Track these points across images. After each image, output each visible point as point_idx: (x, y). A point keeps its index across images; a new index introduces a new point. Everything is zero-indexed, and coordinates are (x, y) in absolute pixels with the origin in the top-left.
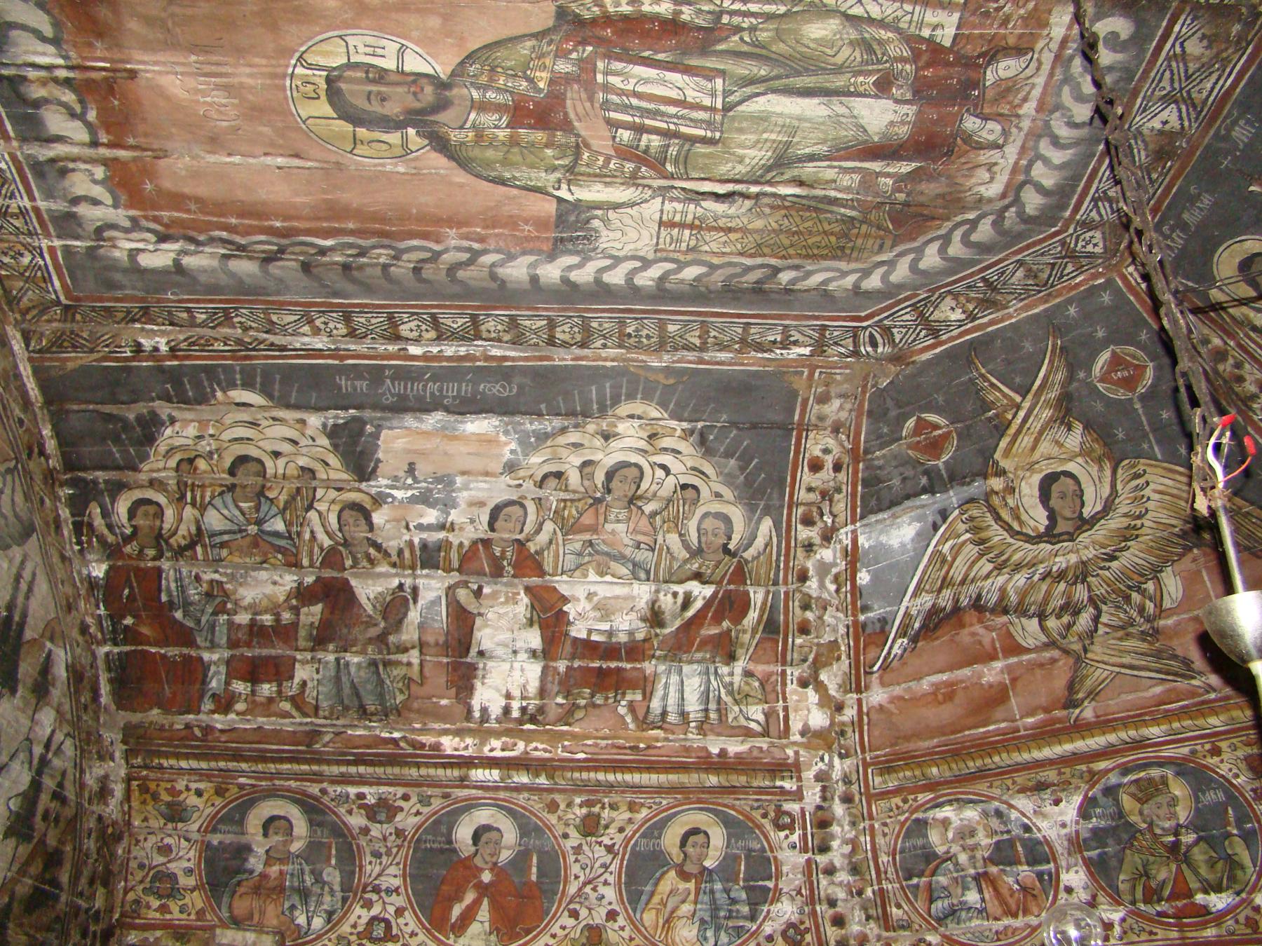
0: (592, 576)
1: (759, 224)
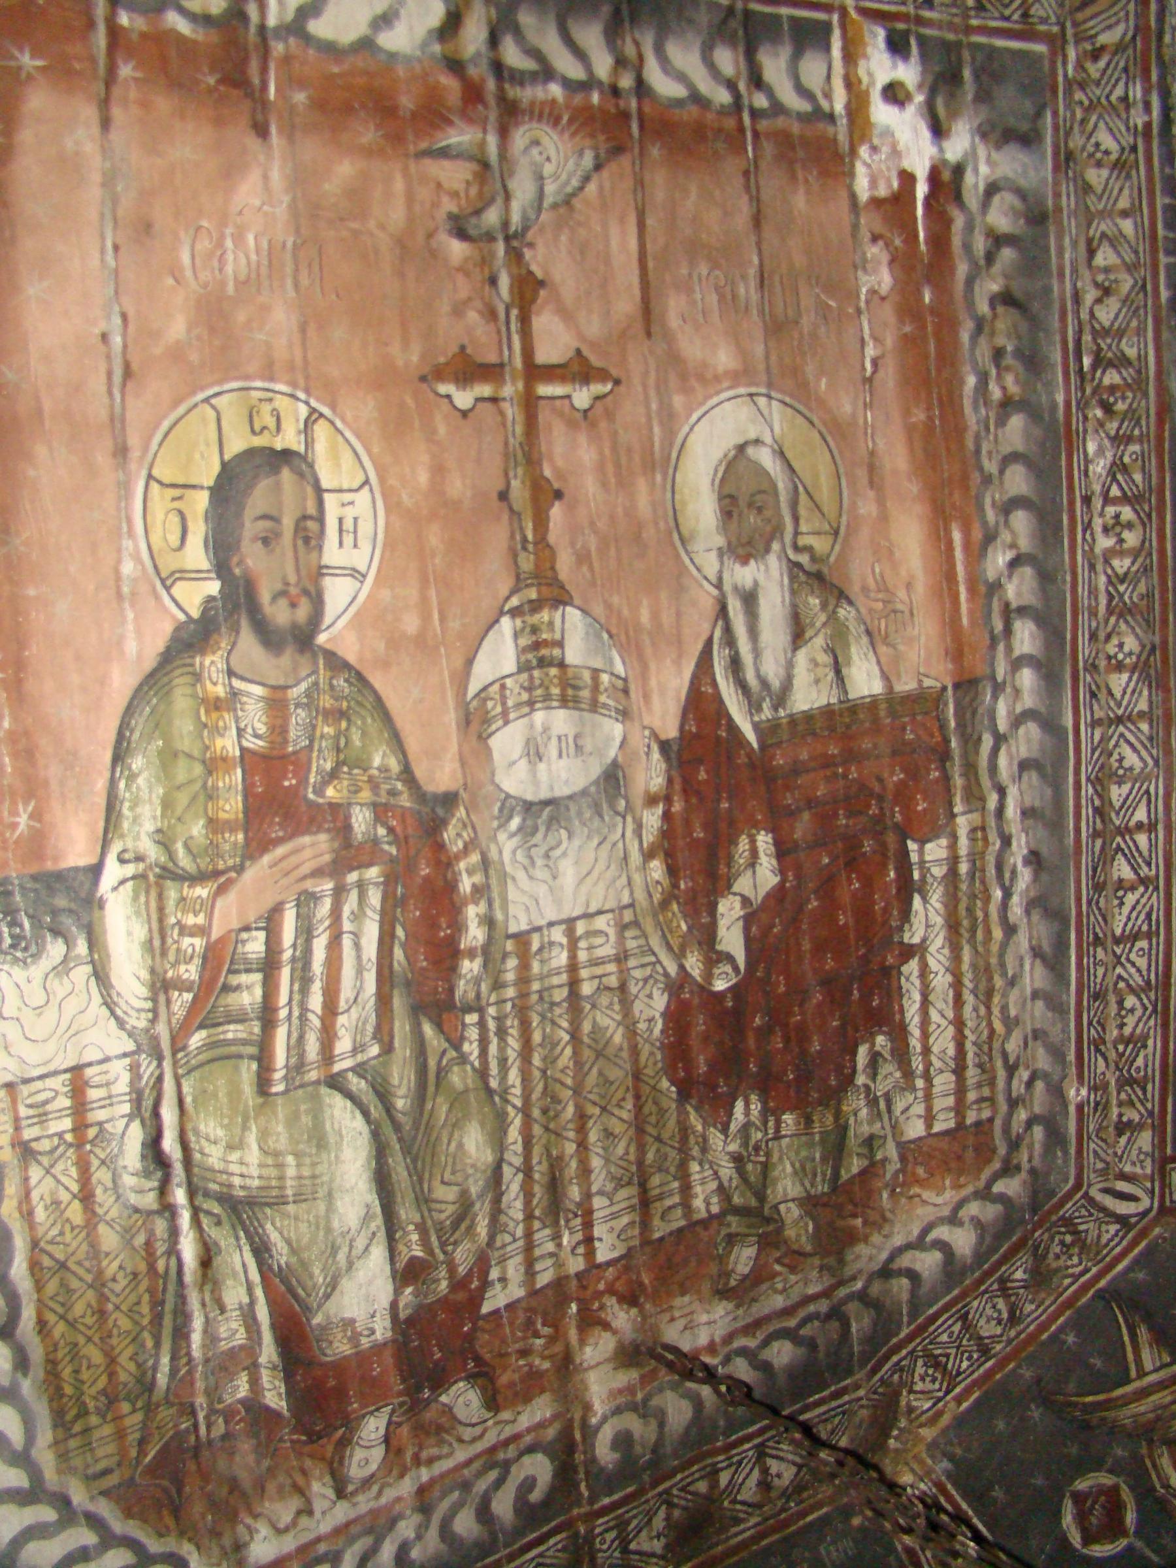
1: (109, 1238)
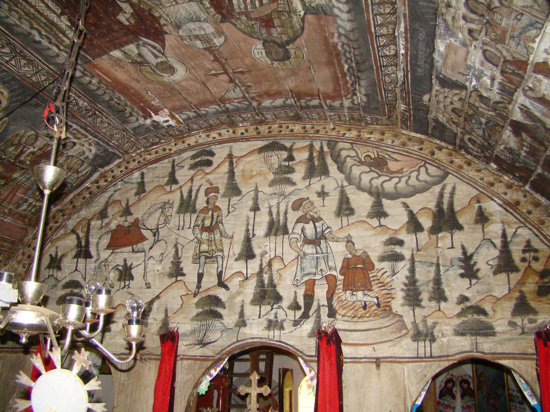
0: (535, 46)
